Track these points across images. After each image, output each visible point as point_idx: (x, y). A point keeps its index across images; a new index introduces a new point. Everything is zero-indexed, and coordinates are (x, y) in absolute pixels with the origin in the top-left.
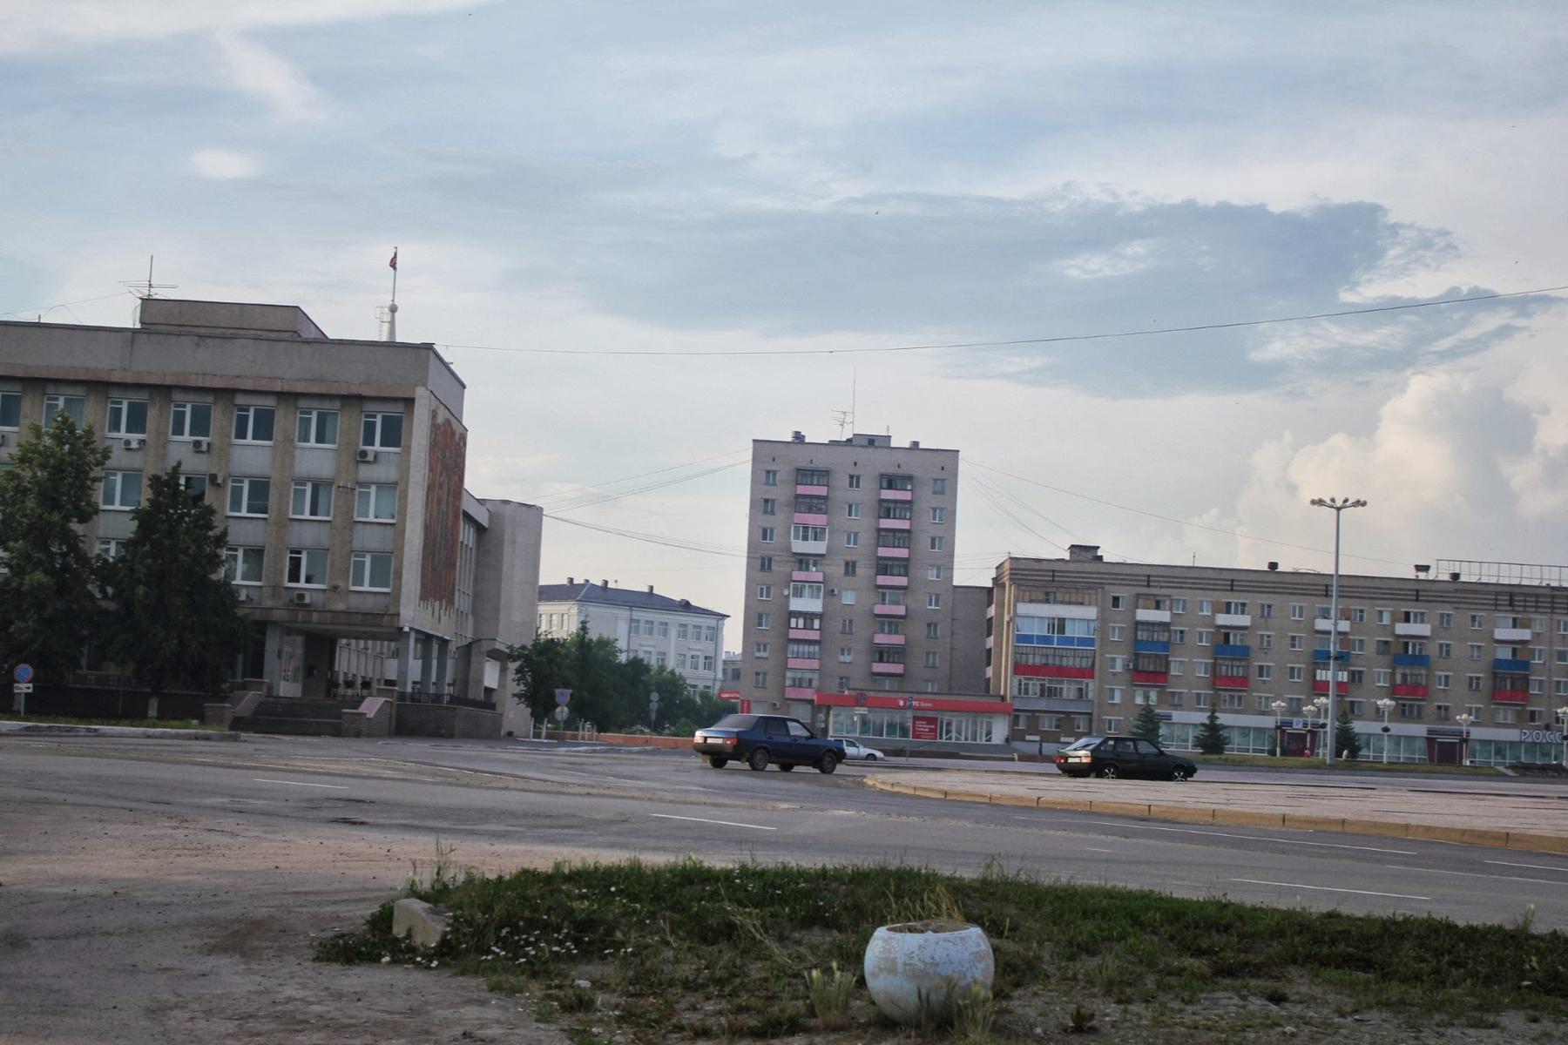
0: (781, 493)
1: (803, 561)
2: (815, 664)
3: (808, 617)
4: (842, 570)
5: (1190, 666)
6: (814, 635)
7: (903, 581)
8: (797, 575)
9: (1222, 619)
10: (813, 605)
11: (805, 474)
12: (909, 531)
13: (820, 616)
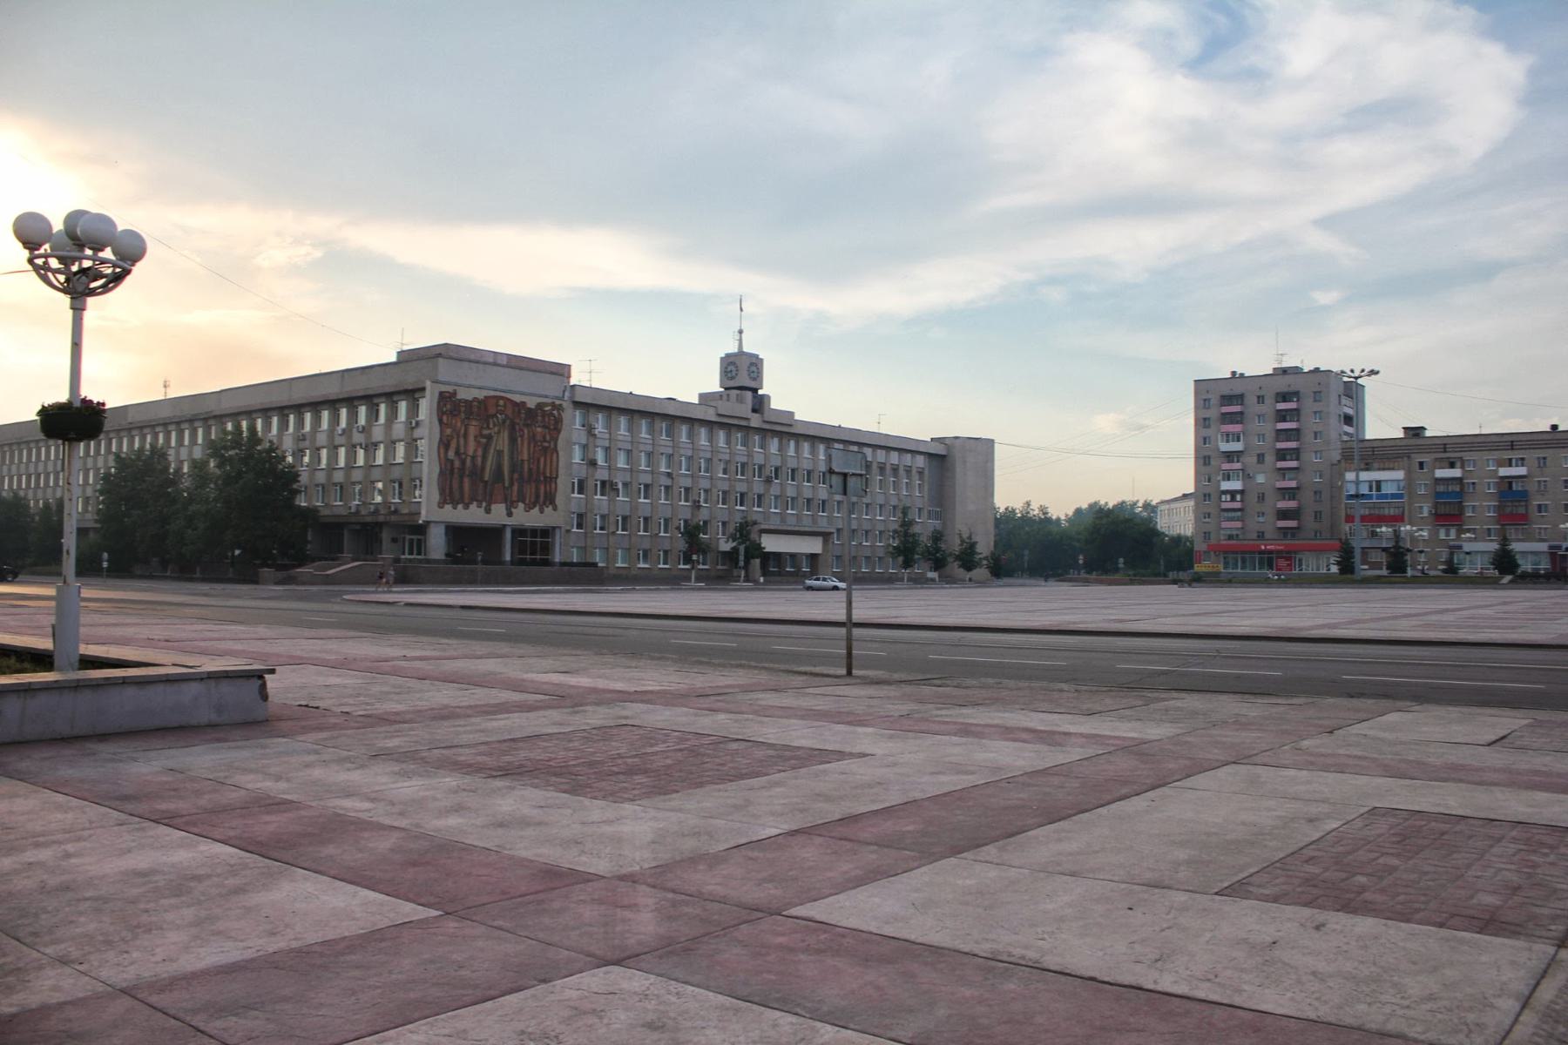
0: (1213, 413)
1: (1230, 456)
2: (1239, 524)
3: (1233, 493)
4: (1255, 459)
5: (1481, 507)
6: (1237, 505)
7: (1294, 464)
8: (1226, 466)
9: (1503, 472)
10: (1236, 485)
11: (1227, 399)
12: (1297, 430)
13: (1242, 492)
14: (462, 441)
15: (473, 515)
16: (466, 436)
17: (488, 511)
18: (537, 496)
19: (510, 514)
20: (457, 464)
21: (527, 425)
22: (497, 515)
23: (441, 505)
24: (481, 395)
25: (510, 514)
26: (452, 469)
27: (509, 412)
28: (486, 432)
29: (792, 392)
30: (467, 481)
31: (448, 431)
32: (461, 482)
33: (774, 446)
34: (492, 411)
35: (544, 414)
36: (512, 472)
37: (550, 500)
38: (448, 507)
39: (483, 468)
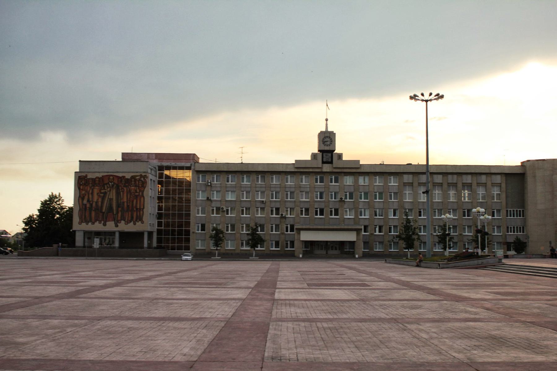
14: (90, 196)
15: (98, 227)
16: (92, 194)
17: (105, 225)
18: (132, 217)
19: (117, 226)
20: (88, 205)
21: (126, 186)
22: (110, 226)
23: (80, 223)
24: (100, 175)
25: (117, 226)
26: (86, 208)
27: (116, 182)
28: (102, 191)
29: (347, 149)
30: (93, 214)
31: (83, 192)
32: (90, 214)
33: (348, 181)
34: (106, 181)
35: (135, 180)
36: (118, 206)
37: (140, 219)
38: (84, 224)
39: (102, 206)
